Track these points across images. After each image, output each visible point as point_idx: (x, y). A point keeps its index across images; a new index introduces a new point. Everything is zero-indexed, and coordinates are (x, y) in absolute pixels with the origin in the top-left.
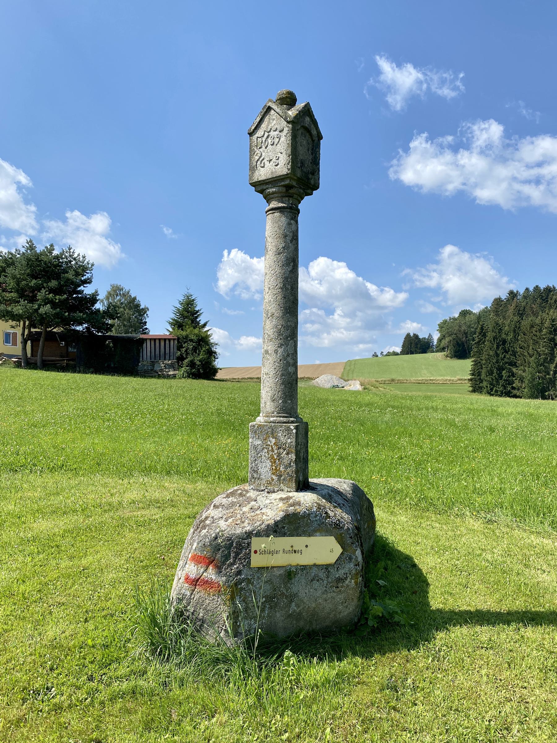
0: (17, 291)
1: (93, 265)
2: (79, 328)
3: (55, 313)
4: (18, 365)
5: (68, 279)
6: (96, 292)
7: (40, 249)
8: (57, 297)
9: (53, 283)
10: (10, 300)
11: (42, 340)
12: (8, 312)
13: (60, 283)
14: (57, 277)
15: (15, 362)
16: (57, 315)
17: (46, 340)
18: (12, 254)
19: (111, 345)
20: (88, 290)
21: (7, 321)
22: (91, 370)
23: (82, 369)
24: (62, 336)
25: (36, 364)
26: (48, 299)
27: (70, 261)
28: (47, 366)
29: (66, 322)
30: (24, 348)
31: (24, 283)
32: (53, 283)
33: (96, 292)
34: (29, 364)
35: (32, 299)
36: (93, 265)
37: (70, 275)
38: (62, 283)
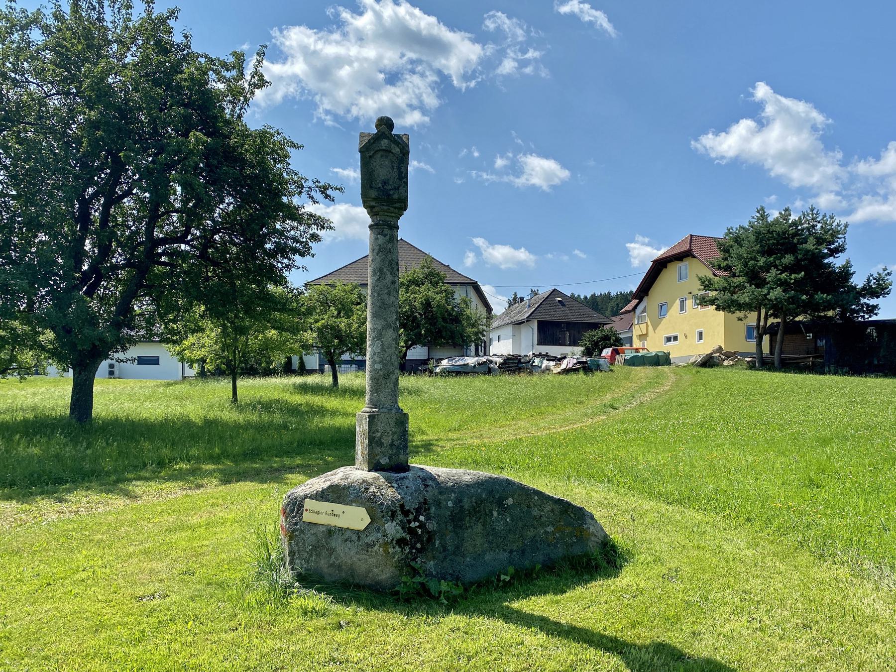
0: (746, 274)
1: (846, 226)
2: (830, 313)
3: (789, 298)
4: (752, 366)
5: (808, 251)
6: (848, 262)
7: (774, 215)
8: (793, 276)
9: (788, 259)
10: (737, 286)
11: (780, 333)
12: (733, 301)
13: (797, 257)
14: (792, 249)
15: (748, 362)
16: (793, 300)
17: (785, 333)
18: (744, 228)
19: (875, 334)
20: (837, 262)
21: (733, 312)
22: (846, 369)
23: (832, 369)
24: (808, 327)
25: (773, 364)
26: (780, 280)
27: (813, 226)
28: (786, 365)
29: (811, 306)
30: (759, 345)
31: (751, 263)
32: (788, 259)
33: (848, 262)
34: (763, 363)
35: (760, 283)
36: (846, 226)
37: (810, 245)
38: (800, 256)
